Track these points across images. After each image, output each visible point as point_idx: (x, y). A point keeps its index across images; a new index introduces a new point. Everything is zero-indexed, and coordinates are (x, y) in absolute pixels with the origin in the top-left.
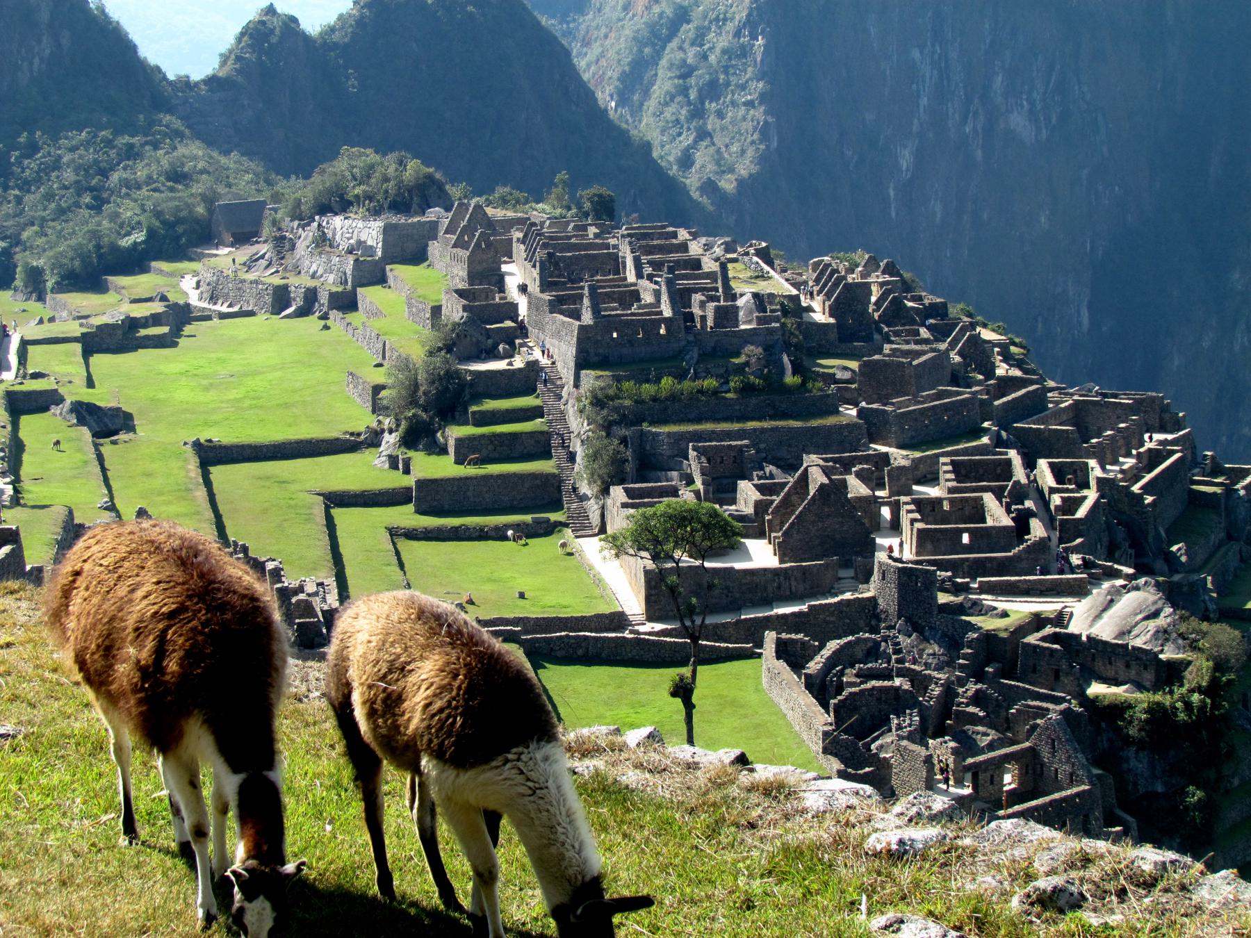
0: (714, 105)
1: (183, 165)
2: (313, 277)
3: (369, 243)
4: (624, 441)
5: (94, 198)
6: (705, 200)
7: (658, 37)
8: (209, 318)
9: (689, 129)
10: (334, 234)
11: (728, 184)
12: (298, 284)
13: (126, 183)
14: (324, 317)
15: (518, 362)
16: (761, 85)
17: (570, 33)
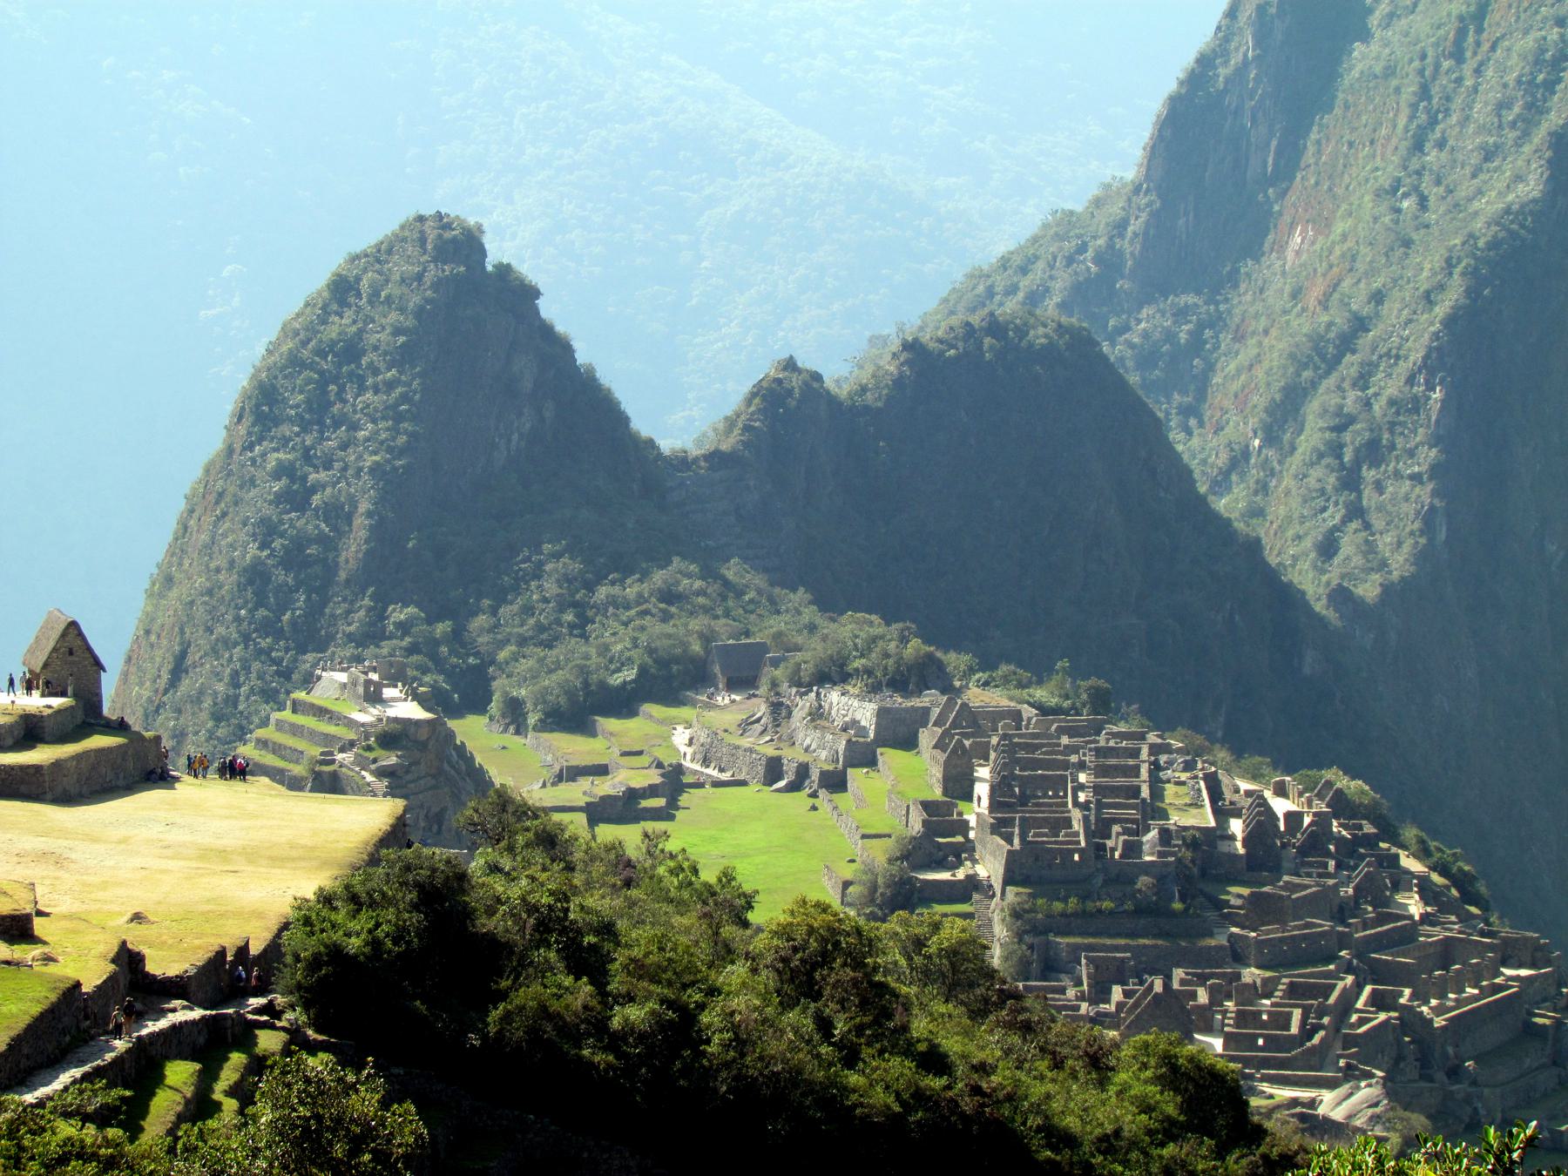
0: (1372, 473)
1: (678, 583)
2: (806, 750)
3: (863, 723)
4: (1031, 947)
5: (576, 616)
6: (1331, 615)
7: (1325, 354)
8: (700, 785)
9: (1336, 503)
10: (831, 708)
11: (1368, 590)
12: (792, 757)
13: (613, 601)
14: (814, 795)
15: (961, 874)
16: (1434, 452)
17: (1220, 318)
